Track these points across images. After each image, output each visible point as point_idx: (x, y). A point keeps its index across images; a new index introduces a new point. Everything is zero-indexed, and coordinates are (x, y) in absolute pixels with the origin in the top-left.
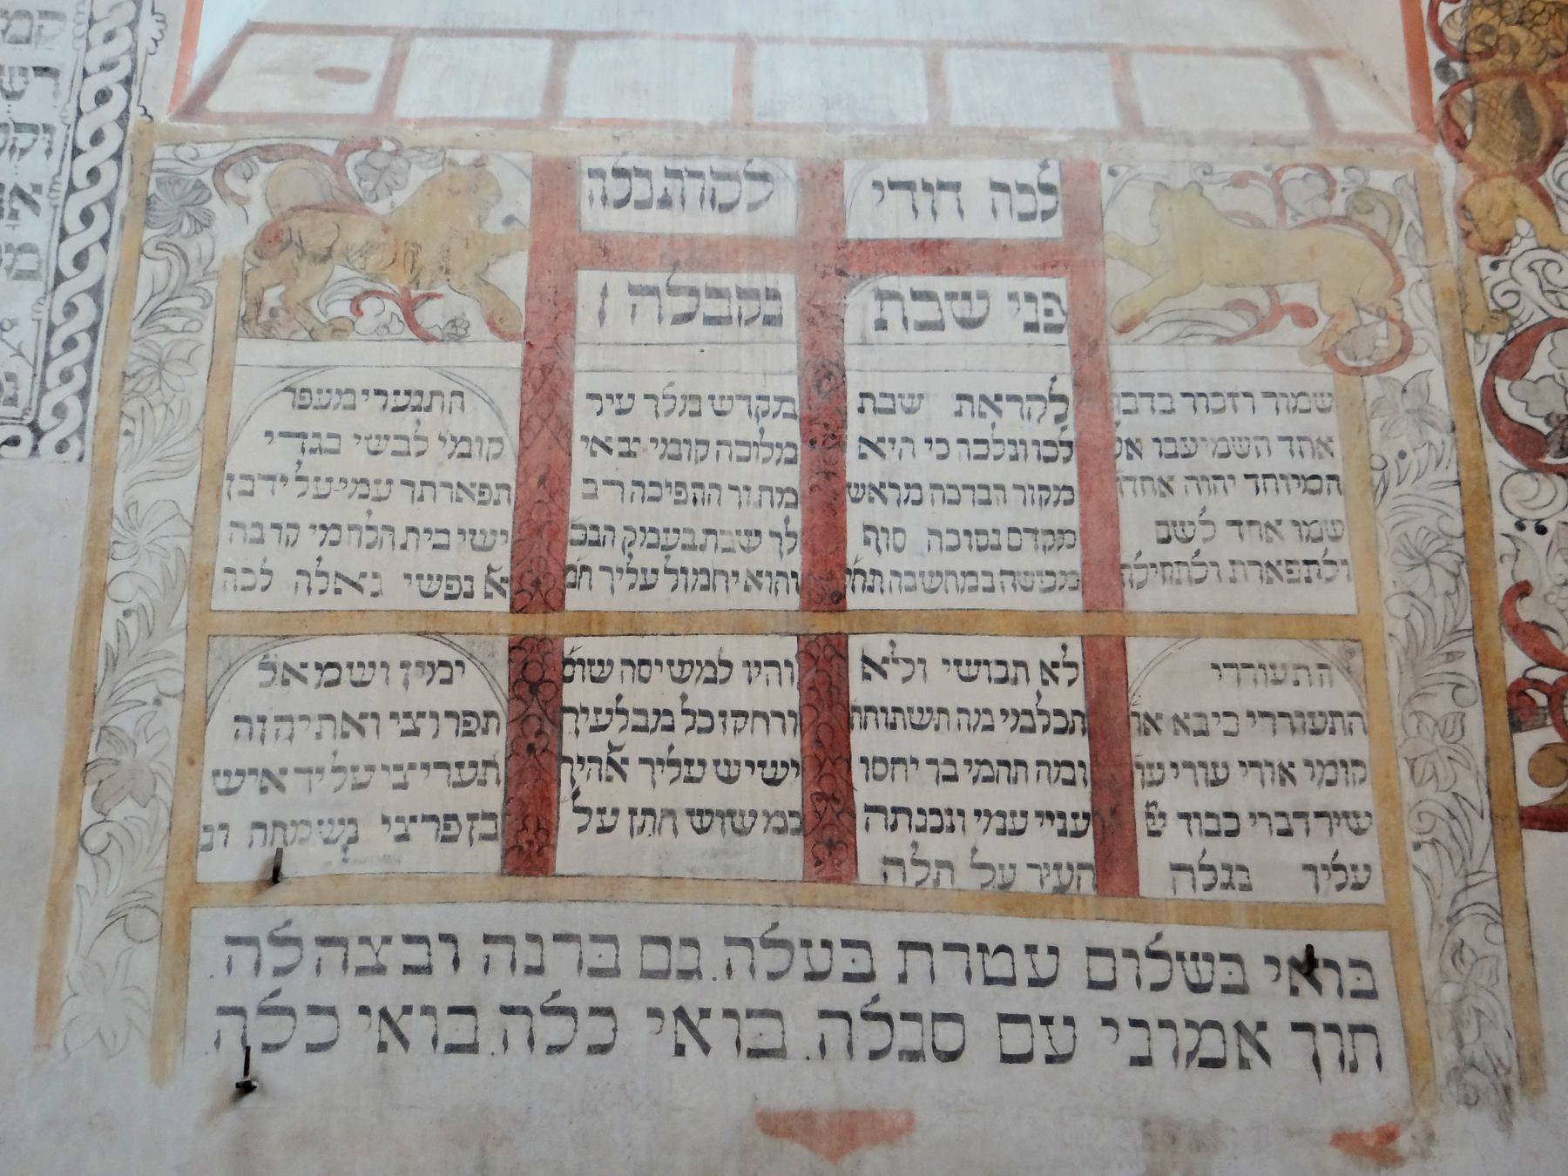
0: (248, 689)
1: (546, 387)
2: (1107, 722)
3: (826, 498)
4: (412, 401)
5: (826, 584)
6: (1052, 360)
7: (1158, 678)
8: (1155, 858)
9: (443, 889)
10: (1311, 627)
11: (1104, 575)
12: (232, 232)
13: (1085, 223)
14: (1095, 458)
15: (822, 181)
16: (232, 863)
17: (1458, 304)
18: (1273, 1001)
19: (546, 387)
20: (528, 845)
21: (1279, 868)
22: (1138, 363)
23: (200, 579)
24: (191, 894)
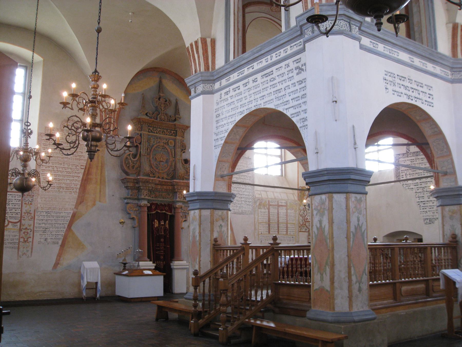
0: (260, 226)
1: (269, 212)
2: (287, 227)
3: (278, 217)
4: (264, 212)
5: (278, 221)
6: (286, 211)
7: (289, 225)
8: (289, 233)
9: (266, 234)
10: (293, 223)
11: (287, 221)
12: (258, 204)
13: (287, 204)
14: (287, 215)
15: (278, 202)
16: (260, 233)
17: (299, 208)
18: (292, 239)
19: (269, 212)
20: (269, 232)
21: (292, 233)
22: (289, 211)
23: (258, 221)
24: (259, 234)
